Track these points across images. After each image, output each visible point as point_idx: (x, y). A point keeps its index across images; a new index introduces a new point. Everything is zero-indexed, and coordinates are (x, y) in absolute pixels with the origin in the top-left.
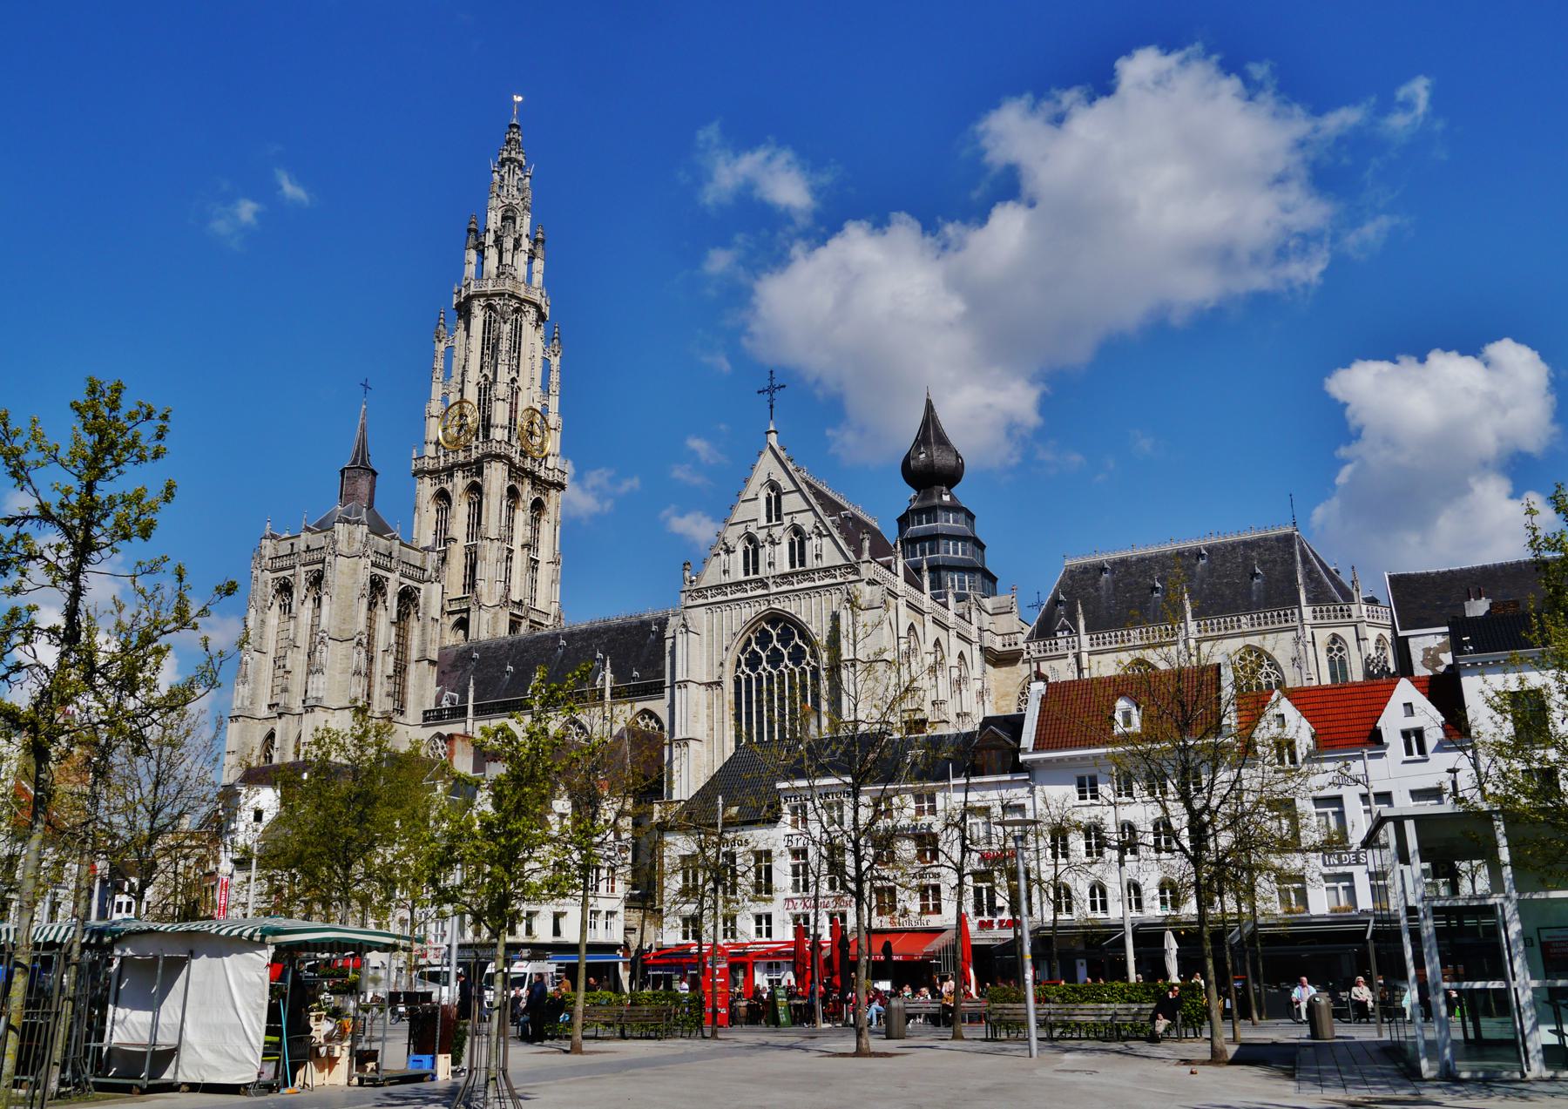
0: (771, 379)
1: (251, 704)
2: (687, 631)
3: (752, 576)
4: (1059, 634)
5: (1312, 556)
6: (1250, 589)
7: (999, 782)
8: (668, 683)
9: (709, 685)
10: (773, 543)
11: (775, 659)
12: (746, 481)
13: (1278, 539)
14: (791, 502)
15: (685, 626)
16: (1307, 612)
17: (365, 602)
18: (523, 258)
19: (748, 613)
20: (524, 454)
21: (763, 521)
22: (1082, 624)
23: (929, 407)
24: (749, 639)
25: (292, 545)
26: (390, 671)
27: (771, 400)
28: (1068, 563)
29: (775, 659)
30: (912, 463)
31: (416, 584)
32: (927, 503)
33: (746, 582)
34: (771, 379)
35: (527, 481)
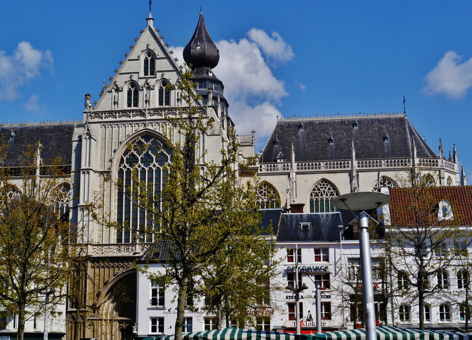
2: (90, 138)
3: (133, 108)
4: (278, 161)
5: (414, 131)
6: (383, 145)
7: (310, 245)
8: (73, 168)
9: (101, 173)
10: (149, 88)
11: (147, 160)
12: (132, 48)
13: (396, 119)
14: (161, 65)
15: (89, 134)
16: (417, 161)
19: (130, 130)
21: (142, 74)
23: (201, 19)
30: (192, 51)
32: (200, 76)
33: (129, 111)
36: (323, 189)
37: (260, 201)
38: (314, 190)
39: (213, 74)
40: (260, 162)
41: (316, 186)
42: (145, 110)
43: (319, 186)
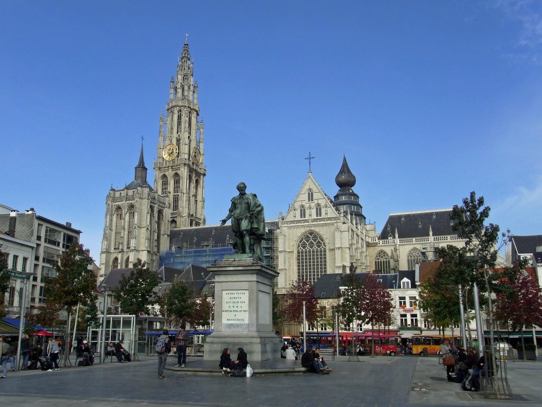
0: (310, 155)
1: (109, 247)
4: (389, 238)
14: (315, 196)
17: (149, 214)
18: (191, 93)
19: (303, 230)
20: (193, 163)
22: (397, 235)
23: (345, 160)
24: (303, 238)
25: (121, 193)
26: (156, 238)
27: (310, 162)
28: (392, 214)
29: (311, 246)
31: (162, 209)
32: (344, 193)
33: (301, 220)
34: (310, 155)
35: (194, 173)
36: (415, 253)
37: (380, 261)
38: (410, 254)
39: (352, 191)
40: (379, 239)
41: (411, 252)
42: (309, 219)
43: (412, 252)
